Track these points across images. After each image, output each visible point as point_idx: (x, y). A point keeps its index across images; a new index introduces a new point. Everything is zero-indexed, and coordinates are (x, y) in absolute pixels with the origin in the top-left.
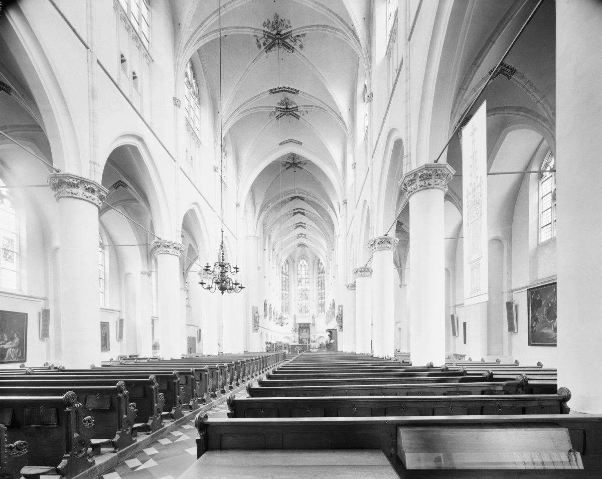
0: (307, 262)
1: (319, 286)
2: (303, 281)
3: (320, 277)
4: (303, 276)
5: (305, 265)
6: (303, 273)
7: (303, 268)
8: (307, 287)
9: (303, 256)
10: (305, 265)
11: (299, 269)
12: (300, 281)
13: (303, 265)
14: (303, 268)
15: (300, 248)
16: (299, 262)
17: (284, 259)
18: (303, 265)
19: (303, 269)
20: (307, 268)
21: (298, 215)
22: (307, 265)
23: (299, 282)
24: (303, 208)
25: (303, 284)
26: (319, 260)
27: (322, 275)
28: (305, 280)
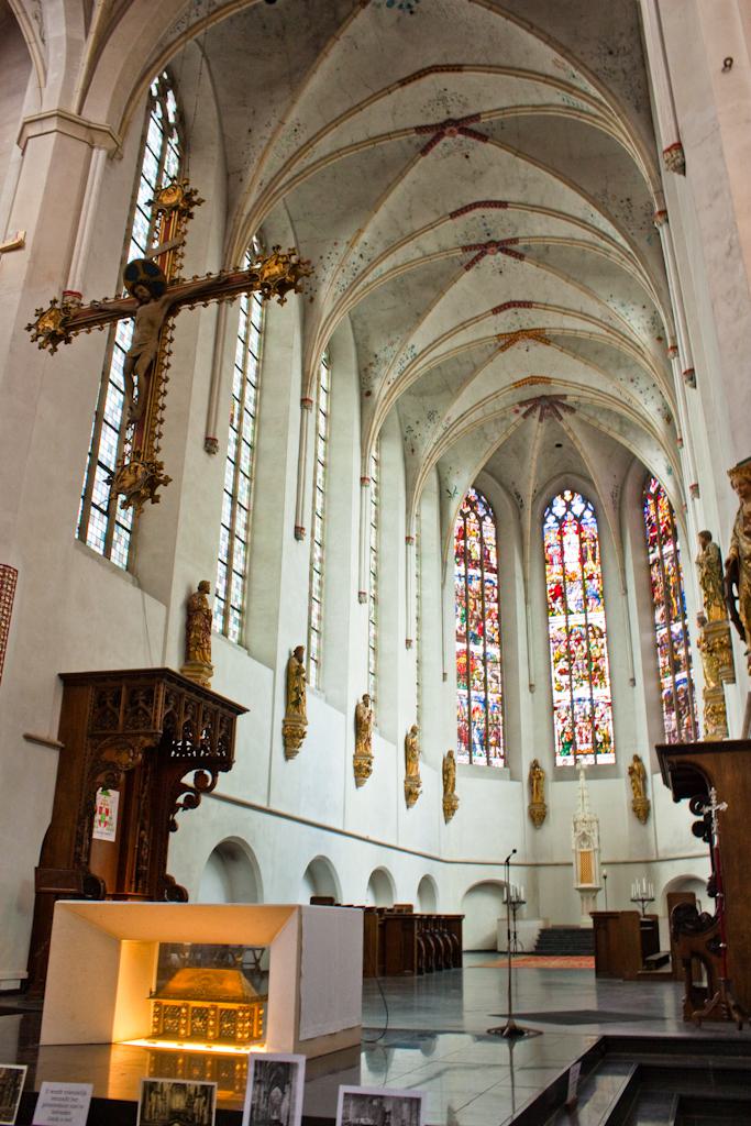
0: (586, 500)
1: (654, 607)
2: (574, 595)
3: (659, 562)
4: (573, 565)
5: (578, 519)
6: (572, 555)
7: (570, 529)
8: (597, 618)
9: (568, 478)
10: (578, 519)
11: (551, 538)
12: (559, 592)
13: (570, 517)
14: (570, 529)
15: (534, 421)
16: (550, 505)
17: (462, 484)
18: (570, 517)
19: (571, 539)
20: (591, 527)
21: (493, 260)
22: (588, 514)
23: (554, 598)
24: (452, 61)
25: (572, 606)
26: (647, 477)
27: (668, 549)
28: (584, 588)
